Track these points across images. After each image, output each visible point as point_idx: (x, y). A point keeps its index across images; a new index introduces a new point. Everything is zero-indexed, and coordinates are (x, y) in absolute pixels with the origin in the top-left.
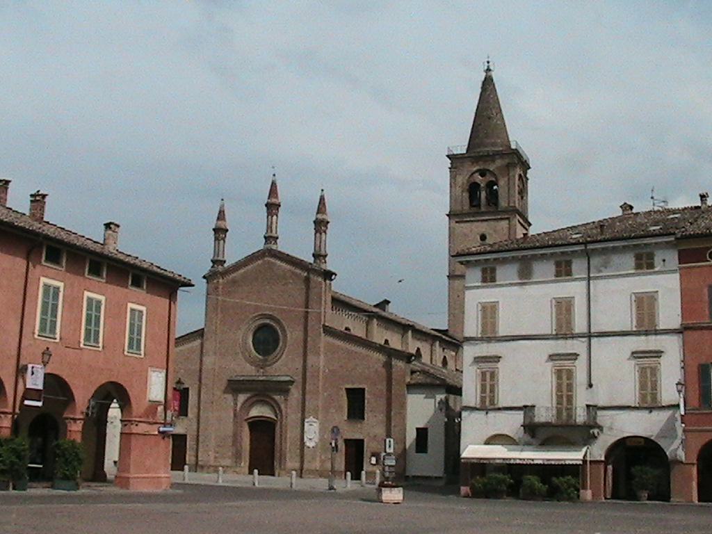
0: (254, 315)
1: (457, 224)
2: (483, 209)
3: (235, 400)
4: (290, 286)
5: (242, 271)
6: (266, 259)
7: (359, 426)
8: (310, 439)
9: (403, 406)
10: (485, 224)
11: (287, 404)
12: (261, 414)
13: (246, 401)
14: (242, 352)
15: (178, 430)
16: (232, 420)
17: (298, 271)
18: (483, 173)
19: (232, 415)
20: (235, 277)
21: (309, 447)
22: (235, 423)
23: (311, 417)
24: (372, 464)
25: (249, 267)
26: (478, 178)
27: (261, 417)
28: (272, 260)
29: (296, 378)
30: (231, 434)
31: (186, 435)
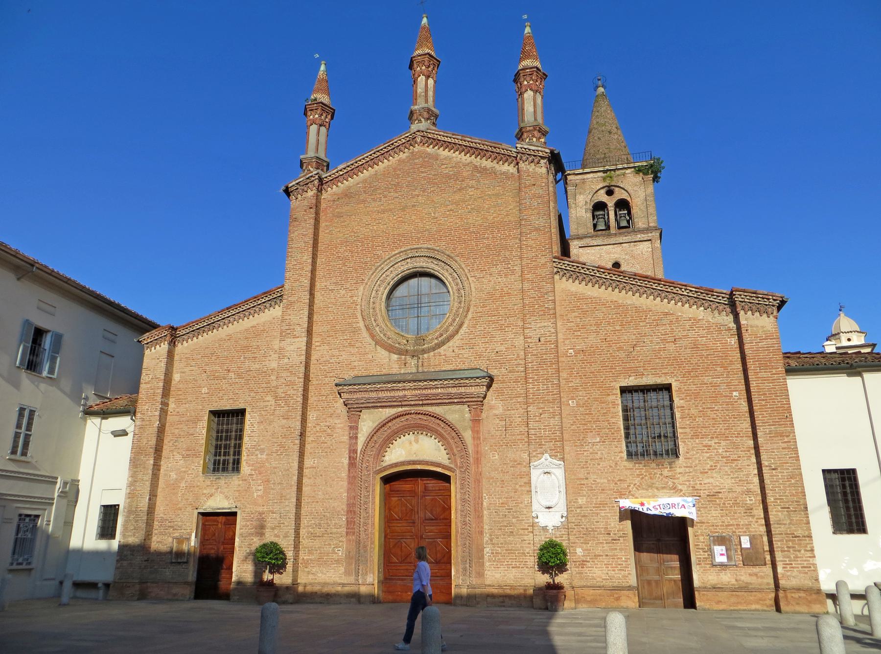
0: (394, 253)
1: (581, 250)
2: (613, 230)
3: (354, 429)
4: (471, 192)
5: (366, 174)
6: (416, 150)
7: (666, 472)
8: (549, 508)
9: (785, 415)
10: (618, 248)
11: (478, 432)
12: (414, 458)
13: (377, 430)
14: (367, 328)
15: (219, 503)
16: (344, 474)
17: (487, 163)
18: (610, 193)
19: (346, 461)
20: (349, 187)
21: (545, 528)
22: (352, 480)
23: (547, 456)
24: (713, 565)
25: (382, 166)
26: (602, 197)
27: (414, 462)
28: (430, 150)
29: (493, 372)
30: (341, 505)
31: (234, 514)
